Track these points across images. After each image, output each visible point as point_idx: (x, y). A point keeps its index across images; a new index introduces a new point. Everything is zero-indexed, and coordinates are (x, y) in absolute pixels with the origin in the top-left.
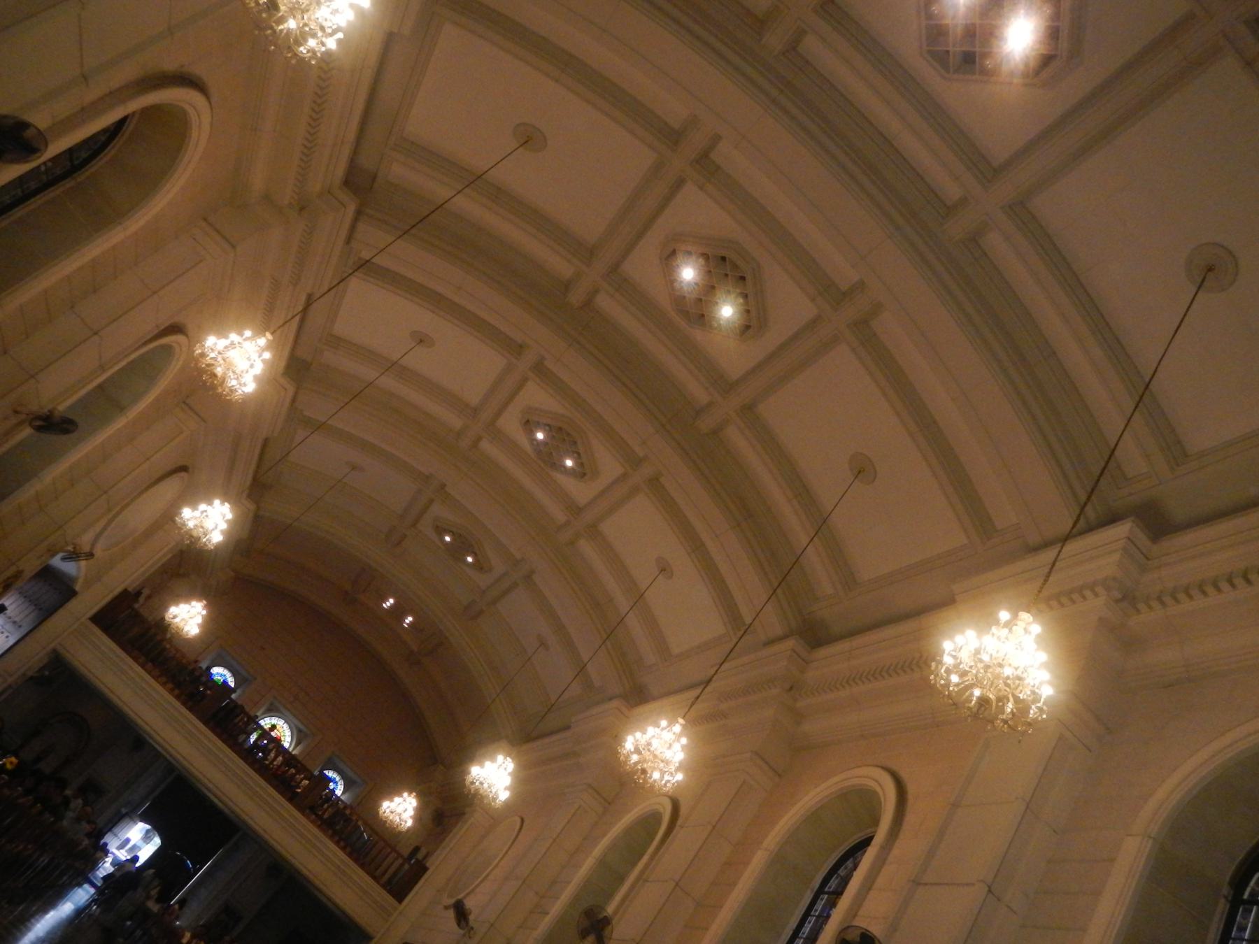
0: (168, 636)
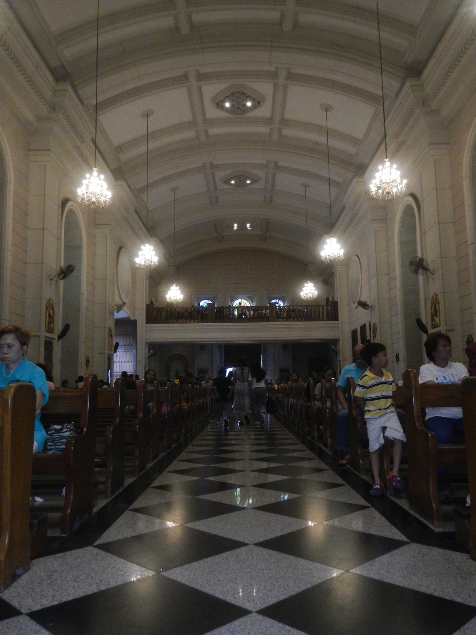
0: (175, 306)
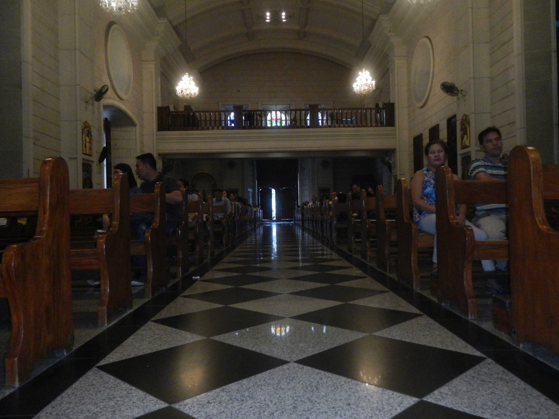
0: (194, 110)
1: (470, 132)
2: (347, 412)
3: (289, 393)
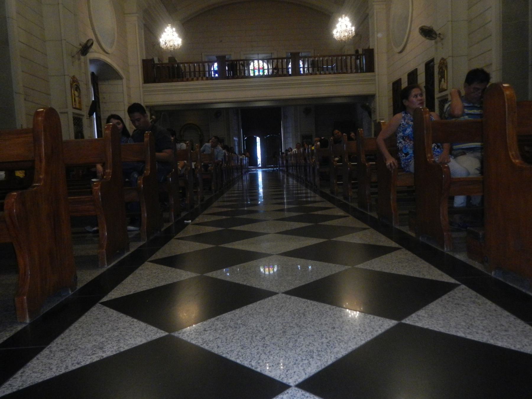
1: (447, 76)
2: (332, 334)
3: (279, 319)
